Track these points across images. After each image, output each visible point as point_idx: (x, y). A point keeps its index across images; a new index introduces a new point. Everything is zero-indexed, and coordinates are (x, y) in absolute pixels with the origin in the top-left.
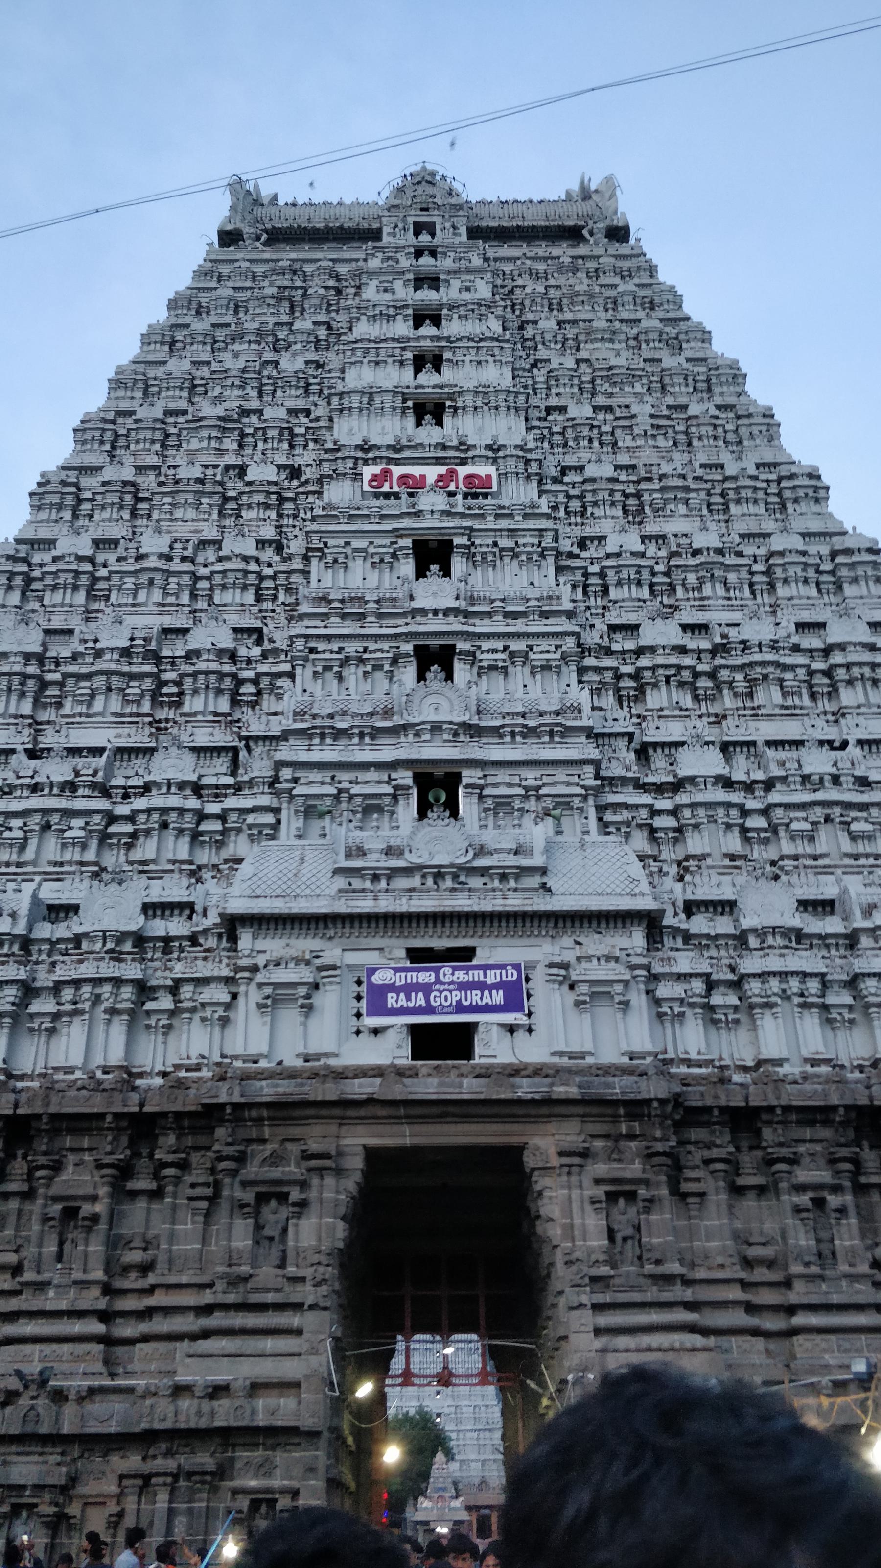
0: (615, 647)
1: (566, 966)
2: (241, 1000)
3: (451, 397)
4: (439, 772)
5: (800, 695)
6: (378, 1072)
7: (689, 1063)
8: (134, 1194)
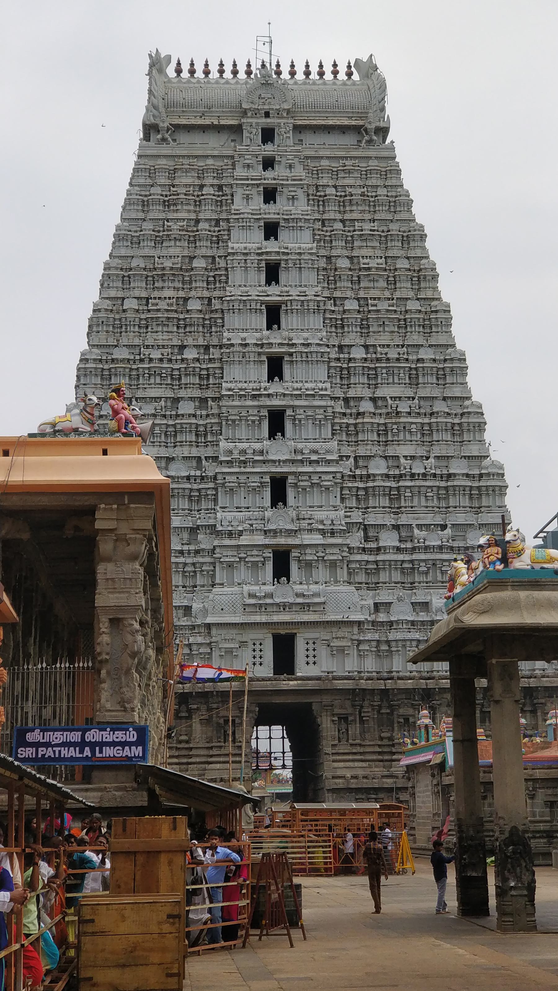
0: (358, 472)
2: (213, 653)
3: (285, 302)
4: (281, 549)
5: (433, 500)
6: (263, 680)
7: (368, 672)
8: (181, 718)
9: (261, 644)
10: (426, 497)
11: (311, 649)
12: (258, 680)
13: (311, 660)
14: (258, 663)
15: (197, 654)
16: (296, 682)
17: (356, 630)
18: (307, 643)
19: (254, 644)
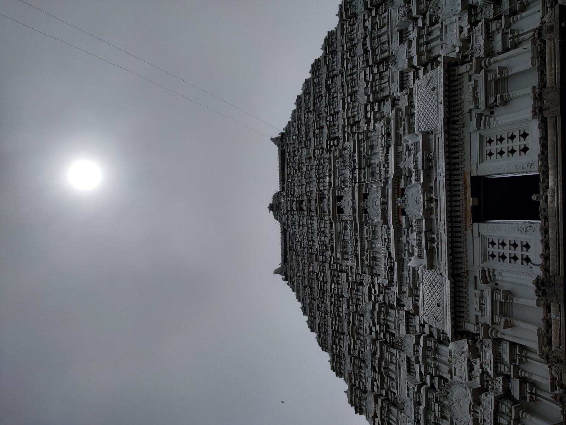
1: (480, 116)
6: (546, 246)
9: (493, 243)
10: (381, 27)
11: (500, 146)
12: (546, 258)
13: (517, 144)
14: (525, 253)
15: (517, 368)
16: (550, 173)
17: (464, 68)
18: (491, 154)
19: (493, 256)
